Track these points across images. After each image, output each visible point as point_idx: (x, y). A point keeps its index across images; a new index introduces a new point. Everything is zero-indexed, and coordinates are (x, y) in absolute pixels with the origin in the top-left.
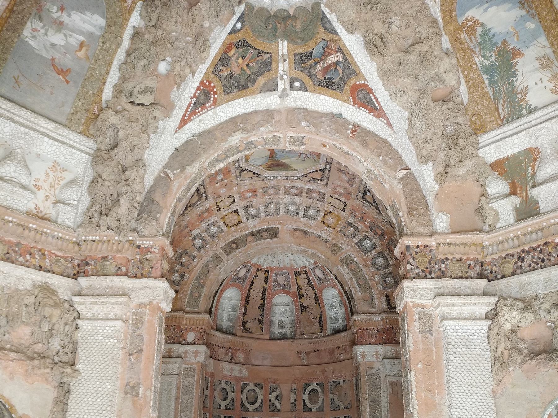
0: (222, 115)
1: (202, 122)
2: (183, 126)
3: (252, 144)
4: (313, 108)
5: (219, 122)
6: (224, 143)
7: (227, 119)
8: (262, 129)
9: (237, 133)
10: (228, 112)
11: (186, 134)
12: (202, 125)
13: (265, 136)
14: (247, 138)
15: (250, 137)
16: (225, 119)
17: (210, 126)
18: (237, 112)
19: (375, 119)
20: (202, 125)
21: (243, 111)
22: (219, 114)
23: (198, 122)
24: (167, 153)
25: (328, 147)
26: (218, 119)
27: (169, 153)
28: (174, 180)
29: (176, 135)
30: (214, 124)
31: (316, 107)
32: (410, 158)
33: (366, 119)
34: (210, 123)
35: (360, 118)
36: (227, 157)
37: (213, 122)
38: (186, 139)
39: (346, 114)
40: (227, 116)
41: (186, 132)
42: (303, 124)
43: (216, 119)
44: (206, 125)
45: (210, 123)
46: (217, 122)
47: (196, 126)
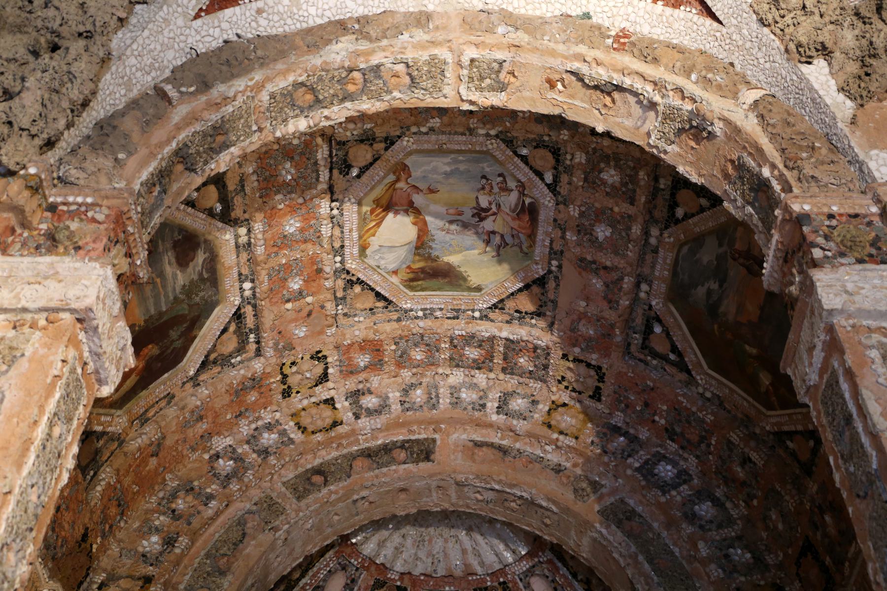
0: (312, 10)
1: (264, 15)
2: (215, 11)
3: (380, 77)
4: (523, 11)
5: (305, 25)
6: (312, 57)
7: (322, 22)
8: (405, 37)
9: (343, 39)
10: (326, 7)
11: (222, 30)
12: (263, 22)
13: (410, 55)
14: (368, 53)
15: (373, 52)
16: (319, 21)
17: (281, 30)
18: (347, 10)
19: (669, 10)
20: (263, 22)
21: (360, 11)
22: (304, 7)
23: (254, 13)
24: (170, 54)
25: (559, 86)
26: (301, 19)
27: (175, 58)
28: (178, 104)
29: (199, 22)
30: (293, 27)
31: (528, 7)
32: (768, 65)
33: (647, 16)
34: (282, 22)
35: (632, 18)
36: (318, 102)
37: (289, 21)
38: (221, 41)
39: (601, 15)
40: (323, 15)
41: (225, 25)
42: (501, 30)
43: (296, 17)
44: (271, 23)
45: (282, 22)
46: (298, 25)
47: (249, 20)
